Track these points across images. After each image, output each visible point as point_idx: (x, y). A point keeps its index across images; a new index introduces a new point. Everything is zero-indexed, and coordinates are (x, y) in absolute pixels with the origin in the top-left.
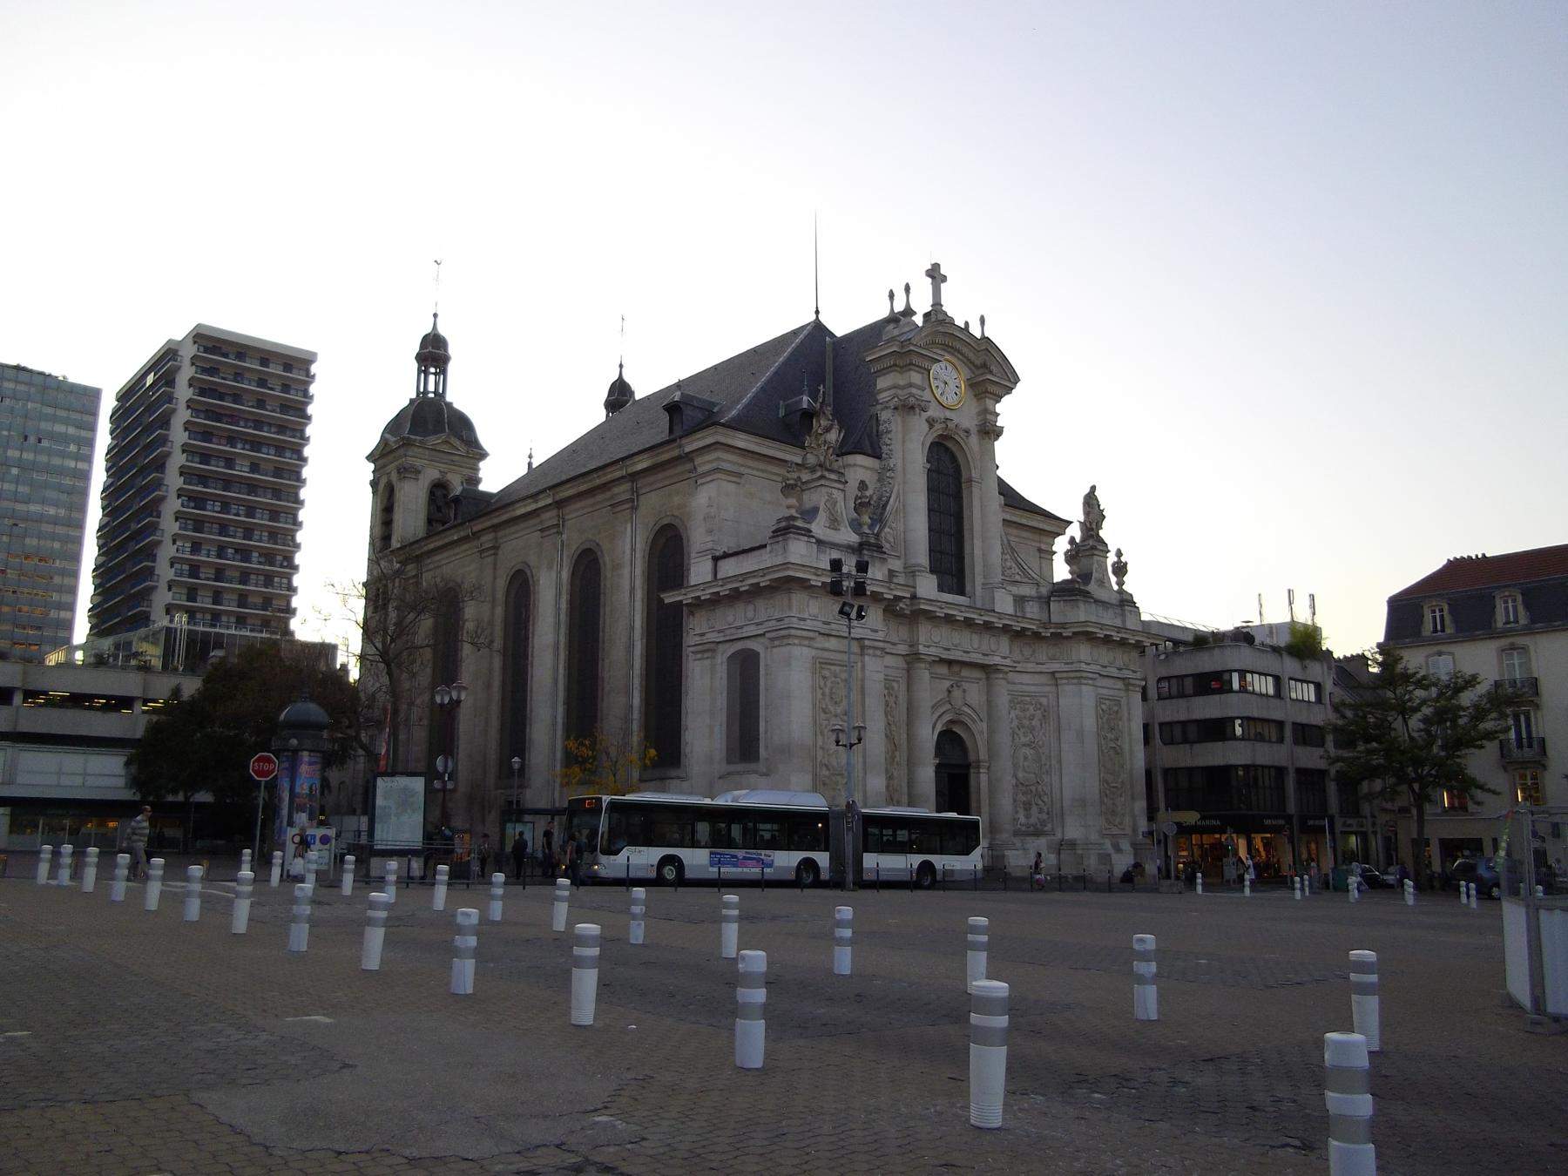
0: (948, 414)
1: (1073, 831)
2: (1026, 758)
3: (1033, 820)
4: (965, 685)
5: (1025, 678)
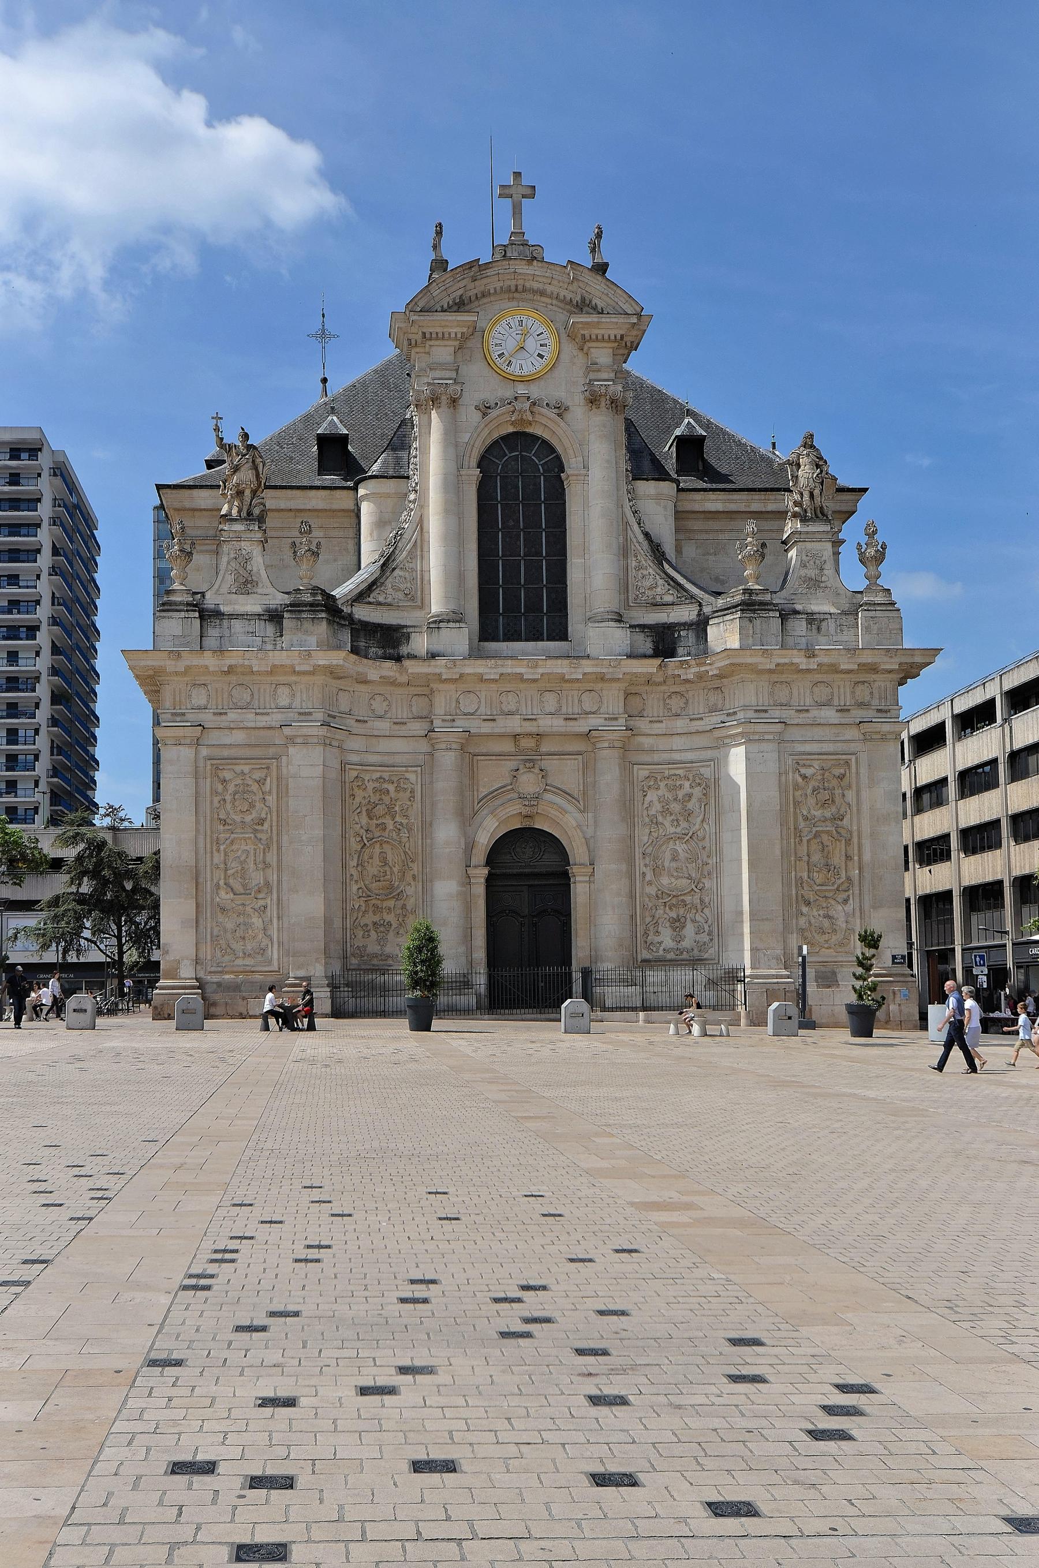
2: (675, 858)
3: (686, 944)
4: (547, 763)
5: (678, 742)
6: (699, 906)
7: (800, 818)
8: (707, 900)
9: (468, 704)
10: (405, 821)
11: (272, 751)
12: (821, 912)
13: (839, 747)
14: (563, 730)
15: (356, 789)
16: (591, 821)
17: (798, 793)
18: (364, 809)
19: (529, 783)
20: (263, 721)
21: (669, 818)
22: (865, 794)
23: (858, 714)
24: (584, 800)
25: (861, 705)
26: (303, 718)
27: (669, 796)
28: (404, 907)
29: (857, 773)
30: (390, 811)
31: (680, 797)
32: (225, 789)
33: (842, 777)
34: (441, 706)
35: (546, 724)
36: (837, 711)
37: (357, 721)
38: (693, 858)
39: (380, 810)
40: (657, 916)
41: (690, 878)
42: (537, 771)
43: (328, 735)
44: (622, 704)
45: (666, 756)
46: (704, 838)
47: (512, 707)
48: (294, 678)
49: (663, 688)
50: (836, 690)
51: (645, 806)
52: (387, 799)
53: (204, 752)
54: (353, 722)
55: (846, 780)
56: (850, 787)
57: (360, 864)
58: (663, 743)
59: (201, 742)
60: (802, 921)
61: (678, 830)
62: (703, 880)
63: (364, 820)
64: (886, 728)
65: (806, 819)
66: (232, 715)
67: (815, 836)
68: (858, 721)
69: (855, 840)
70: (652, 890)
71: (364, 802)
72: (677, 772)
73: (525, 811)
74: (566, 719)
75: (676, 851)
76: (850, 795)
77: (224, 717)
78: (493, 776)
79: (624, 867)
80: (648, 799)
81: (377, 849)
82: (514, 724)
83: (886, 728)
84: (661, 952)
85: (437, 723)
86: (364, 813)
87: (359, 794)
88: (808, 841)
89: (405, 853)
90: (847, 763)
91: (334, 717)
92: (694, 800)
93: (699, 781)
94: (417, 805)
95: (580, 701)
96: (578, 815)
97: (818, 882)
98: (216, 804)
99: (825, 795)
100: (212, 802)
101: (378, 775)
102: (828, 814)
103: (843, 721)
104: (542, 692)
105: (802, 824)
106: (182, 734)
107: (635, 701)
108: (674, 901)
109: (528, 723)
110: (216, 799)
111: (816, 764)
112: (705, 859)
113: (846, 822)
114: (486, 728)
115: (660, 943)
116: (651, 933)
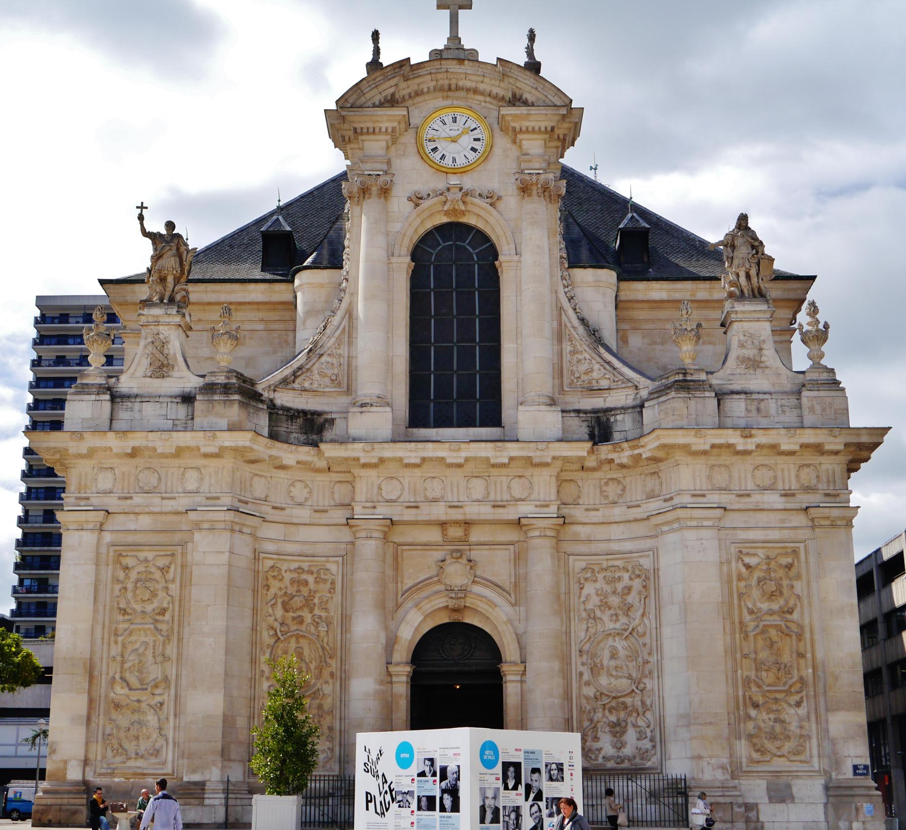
0: (454, 180)
1: (678, 766)
4: (475, 554)
5: (616, 532)
6: (640, 709)
7: (745, 612)
8: (648, 702)
9: (391, 490)
10: (324, 614)
11: (177, 537)
12: (772, 716)
13: (786, 534)
14: (491, 517)
15: (271, 580)
16: (523, 616)
17: (743, 584)
18: (279, 601)
19: (456, 574)
20: (169, 505)
21: (608, 613)
22: (814, 585)
23: (805, 499)
24: (516, 592)
25: (808, 489)
26: (211, 502)
27: (608, 588)
28: (320, 707)
29: (807, 562)
30: (308, 604)
31: (619, 590)
32: (127, 577)
33: (789, 567)
34: (362, 491)
35: (473, 511)
36: (781, 495)
37: (274, 508)
38: (633, 656)
39: (298, 601)
40: (596, 719)
41: (630, 677)
42: (464, 561)
43: (237, 520)
44: (554, 490)
45: (604, 547)
46: (644, 634)
47: (437, 493)
48: (203, 462)
49: (597, 474)
50: (779, 474)
51: (583, 599)
52: (305, 591)
53: (108, 537)
54: (269, 510)
55: (793, 572)
56: (798, 577)
57: (273, 660)
58: (600, 532)
59: (105, 527)
60: (750, 725)
61: (618, 626)
62: (645, 680)
63: (279, 612)
64: (835, 513)
65: (751, 612)
66: (138, 499)
67: (763, 632)
68: (804, 506)
69: (807, 635)
70: (590, 691)
71: (280, 593)
72: (616, 563)
73: (452, 604)
74: (494, 506)
75: (615, 648)
76: (799, 587)
77: (129, 502)
78: (418, 567)
79: (556, 665)
80: (585, 592)
81: (293, 644)
82: (440, 512)
83: (835, 513)
84: (600, 760)
85: (358, 510)
86: (279, 606)
87: (275, 585)
88: (755, 636)
89: (323, 648)
90: (795, 552)
91: (246, 503)
92: (634, 593)
93: (638, 573)
94: (337, 598)
95: (509, 488)
96: (508, 609)
97: (767, 681)
98: (117, 592)
99: (771, 586)
100: (112, 590)
101: (296, 565)
102: (775, 606)
103: (788, 506)
104: (469, 477)
105: (747, 617)
106: (84, 519)
107: (569, 489)
108: (614, 703)
109: (453, 511)
110: (117, 587)
111: (761, 552)
112: (646, 657)
113: (795, 616)
114: (410, 515)
115: (600, 750)
116: (589, 739)
